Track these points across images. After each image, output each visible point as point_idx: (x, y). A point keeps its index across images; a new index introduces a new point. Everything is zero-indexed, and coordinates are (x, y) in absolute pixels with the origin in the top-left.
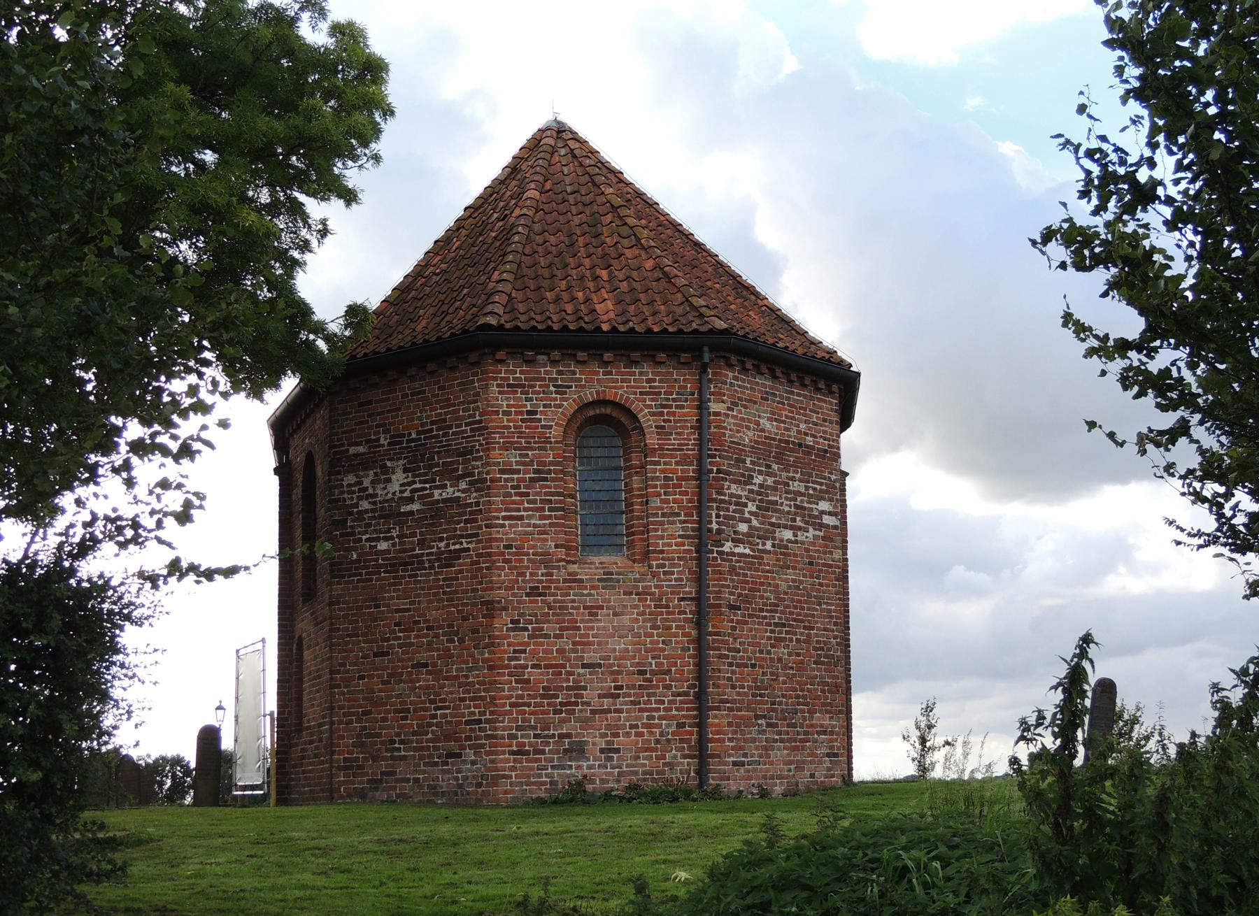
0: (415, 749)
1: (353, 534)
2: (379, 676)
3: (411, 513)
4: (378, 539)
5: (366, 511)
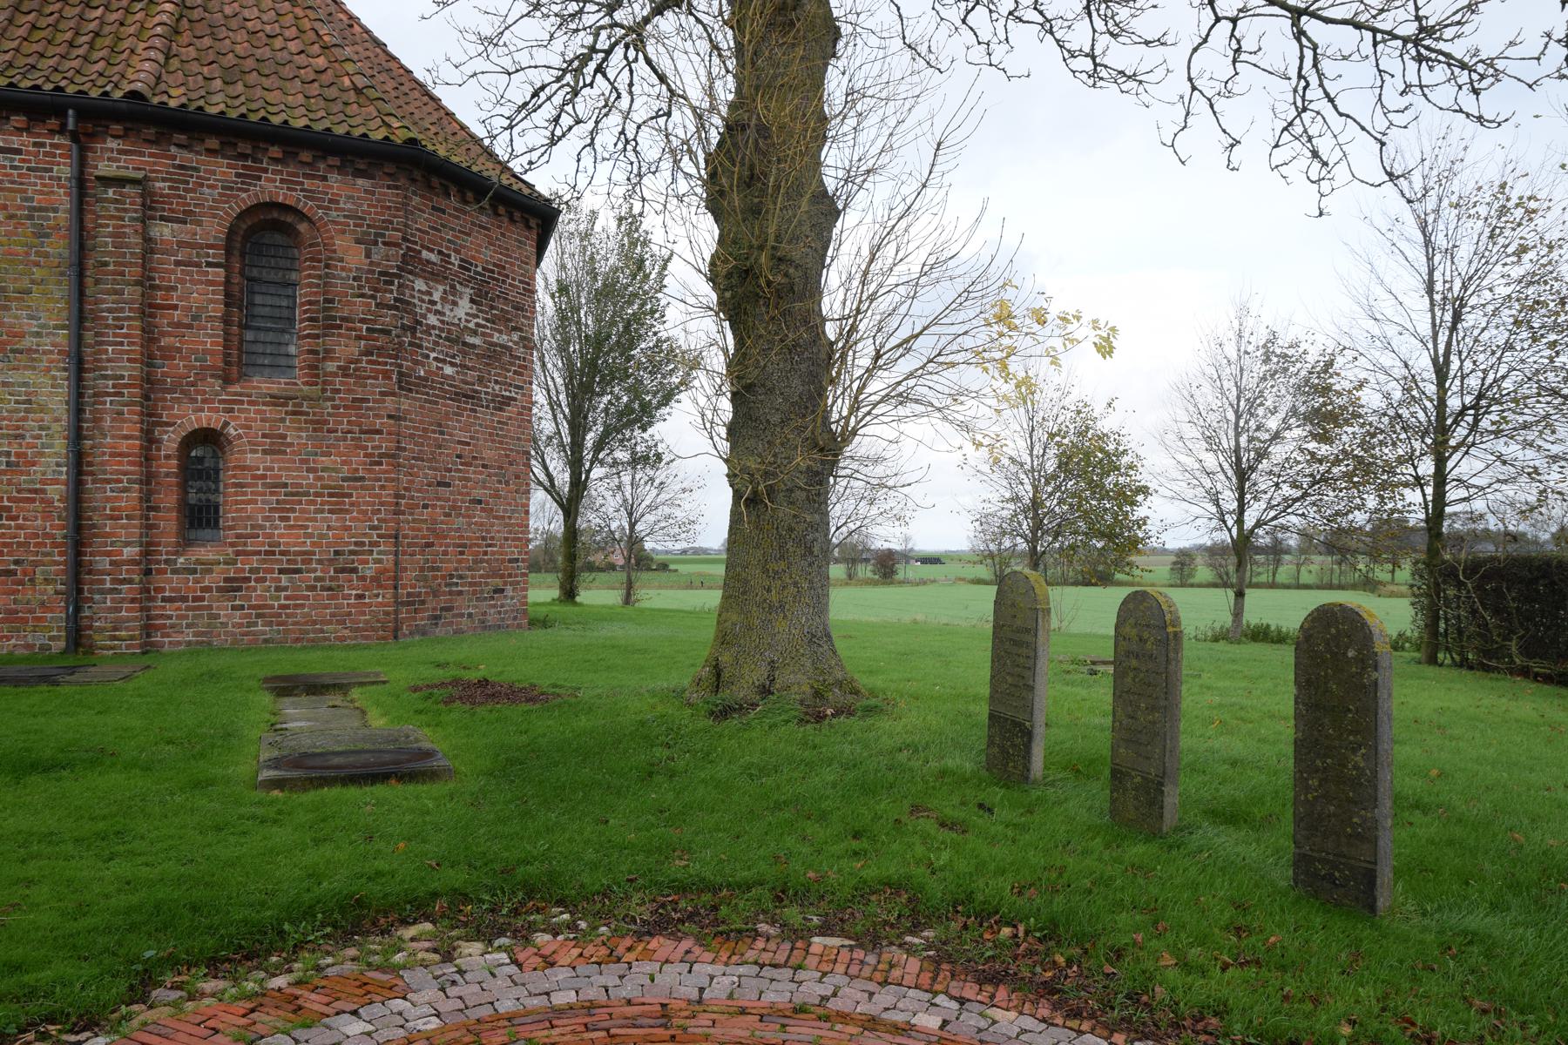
0: (471, 584)
1: (420, 347)
2: (442, 507)
3: (474, 346)
4: (444, 361)
5: (434, 327)
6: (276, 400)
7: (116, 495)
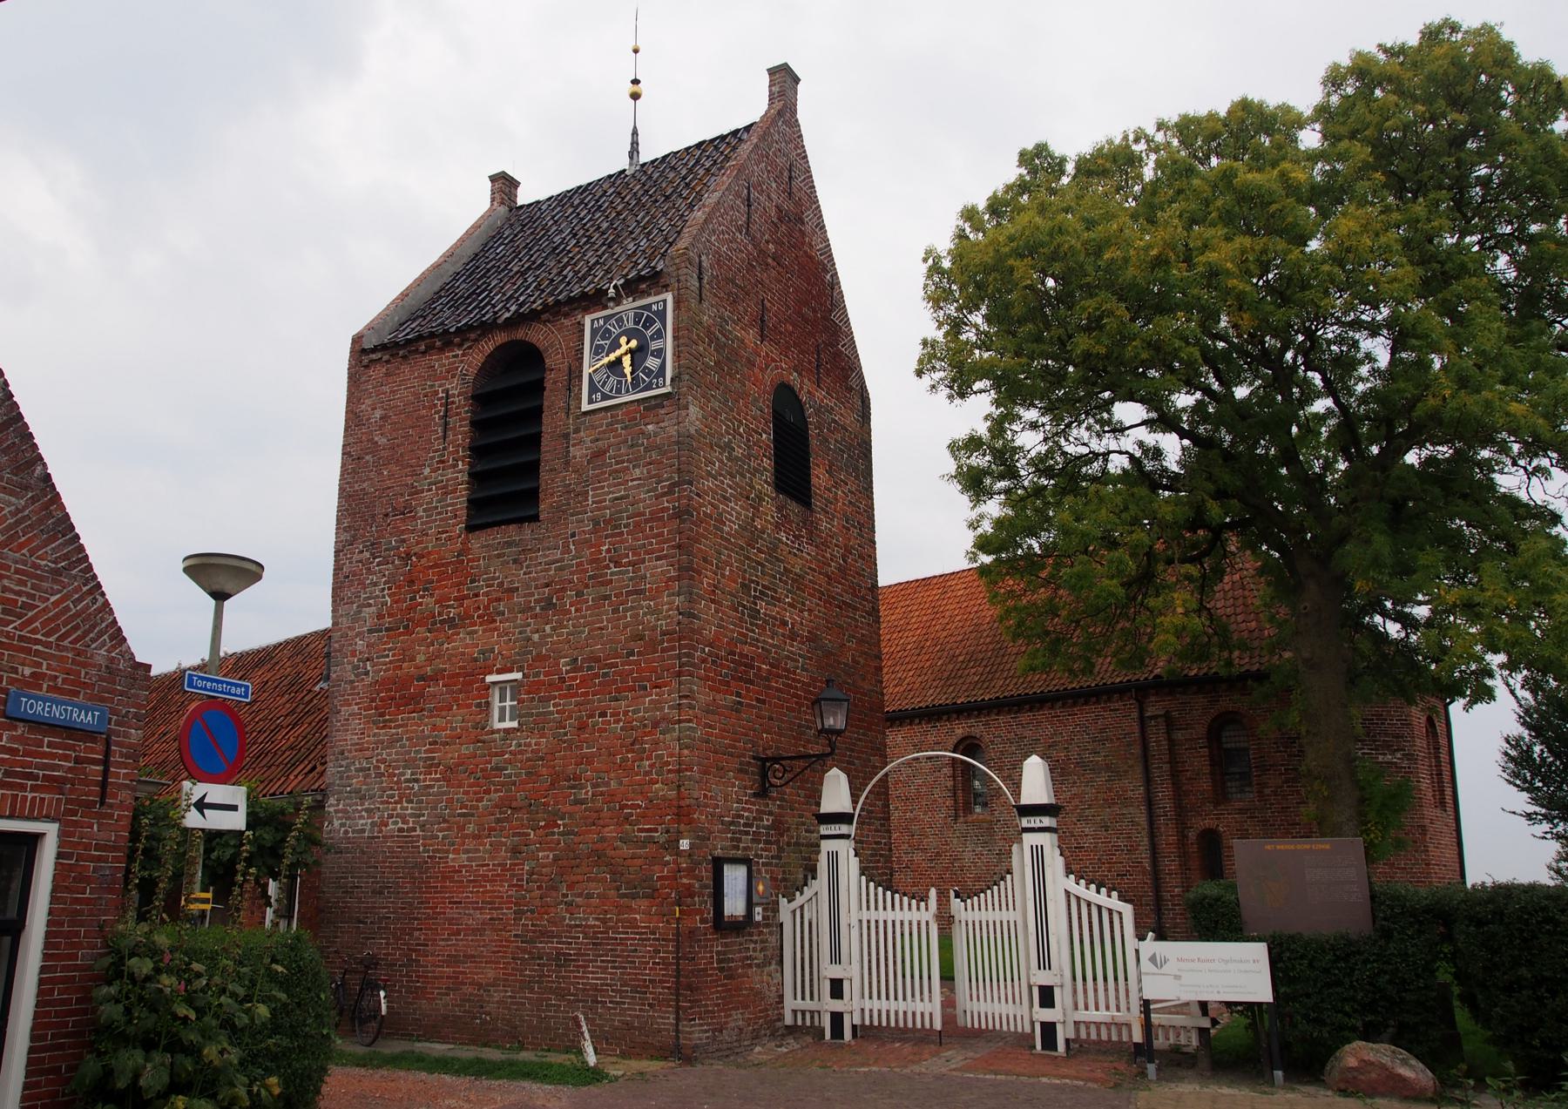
6: (1241, 811)
7: (1170, 864)
